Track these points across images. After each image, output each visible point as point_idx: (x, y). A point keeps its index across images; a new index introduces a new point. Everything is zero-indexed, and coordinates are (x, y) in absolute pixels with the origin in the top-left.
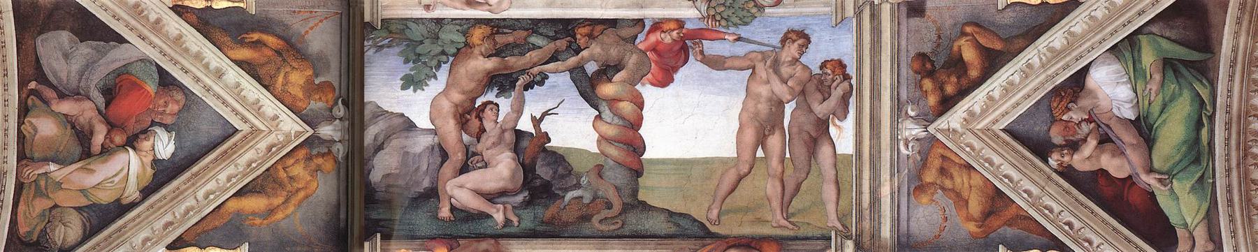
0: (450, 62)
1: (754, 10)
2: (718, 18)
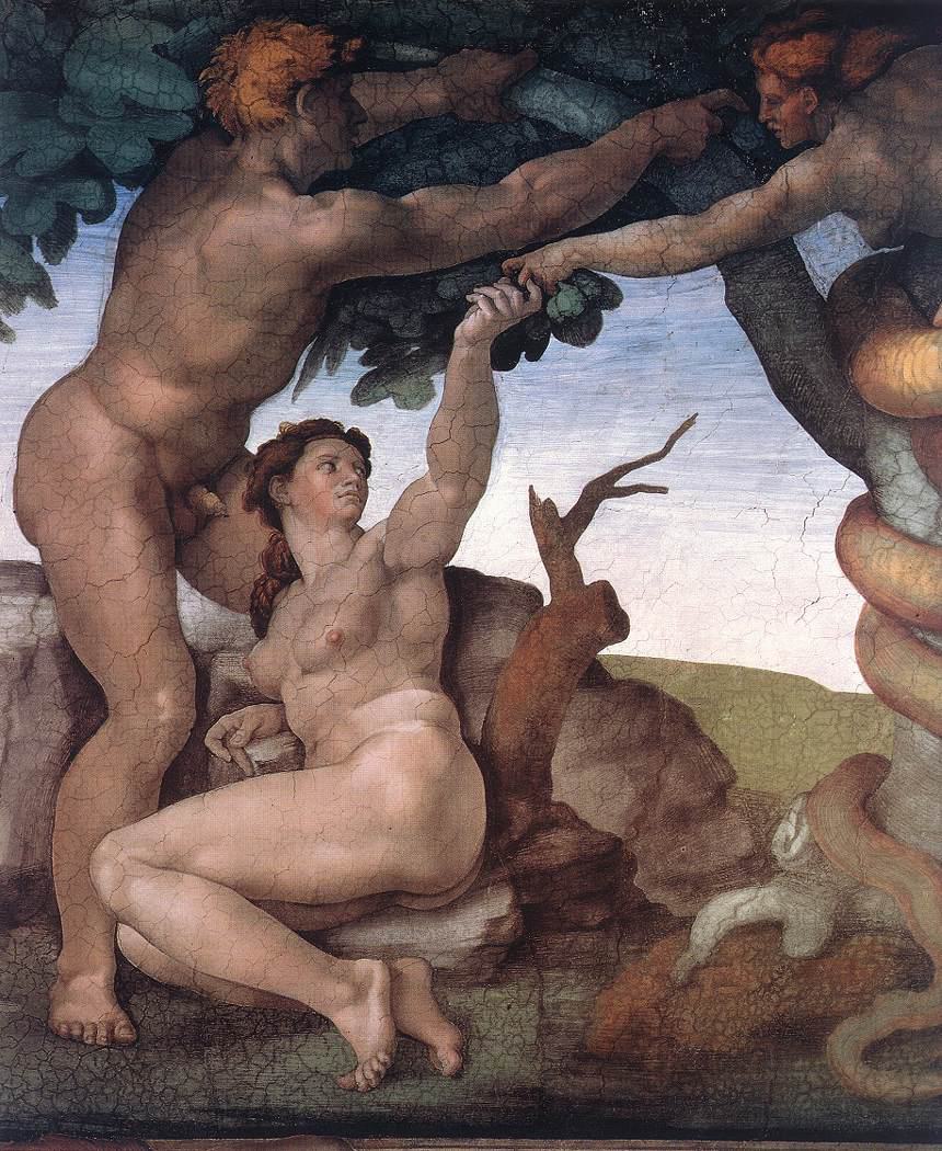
0: (119, 213)
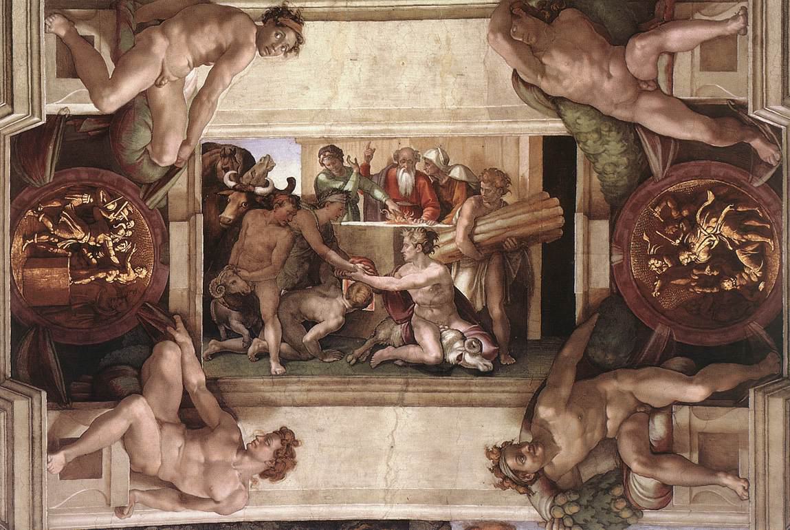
1: (626, 514)
2: (568, 523)
